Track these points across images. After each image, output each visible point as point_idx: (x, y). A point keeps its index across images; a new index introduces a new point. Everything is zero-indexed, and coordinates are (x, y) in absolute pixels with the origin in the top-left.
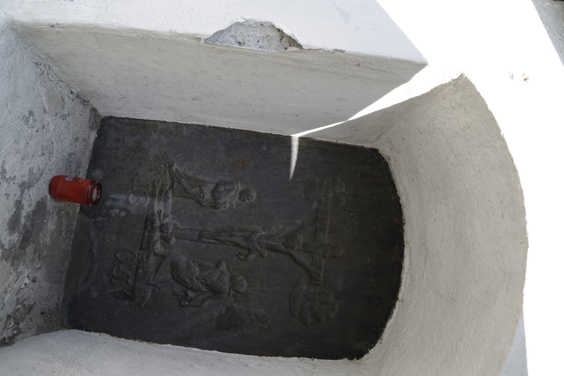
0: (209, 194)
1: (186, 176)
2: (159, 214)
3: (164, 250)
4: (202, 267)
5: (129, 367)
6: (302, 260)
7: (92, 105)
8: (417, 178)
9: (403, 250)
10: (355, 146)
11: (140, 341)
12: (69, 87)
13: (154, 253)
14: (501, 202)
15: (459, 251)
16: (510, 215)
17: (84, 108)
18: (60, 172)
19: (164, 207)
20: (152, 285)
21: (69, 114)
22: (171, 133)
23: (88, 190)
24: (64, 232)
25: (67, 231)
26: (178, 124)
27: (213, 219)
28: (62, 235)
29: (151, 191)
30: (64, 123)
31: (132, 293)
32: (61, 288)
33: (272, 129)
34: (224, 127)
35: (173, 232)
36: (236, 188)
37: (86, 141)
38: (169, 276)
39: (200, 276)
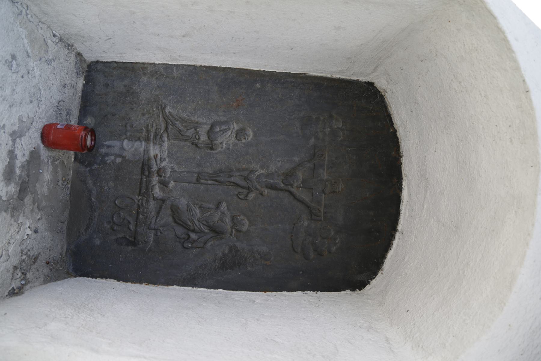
0: (204, 135)
1: (180, 118)
2: (155, 159)
3: (163, 194)
4: (202, 208)
5: (139, 309)
6: (303, 197)
7: (77, 49)
8: (416, 108)
9: (402, 182)
10: (350, 79)
11: (146, 285)
12: (51, 29)
13: (154, 197)
14: (510, 126)
15: (463, 179)
16: (519, 139)
17: (68, 52)
18: (51, 120)
19: (160, 150)
20: (154, 229)
21: (54, 59)
22: (161, 75)
23: (82, 136)
24: (61, 182)
25: (64, 181)
26: (167, 65)
27: (211, 160)
28: (59, 185)
29: (146, 136)
30: (50, 68)
31: (135, 238)
32: (63, 237)
33: (265, 66)
34: (216, 66)
35: (170, 176)
36: (232, 127)
37: (74, 88)
38: (171, 219)
39: (201, 218)
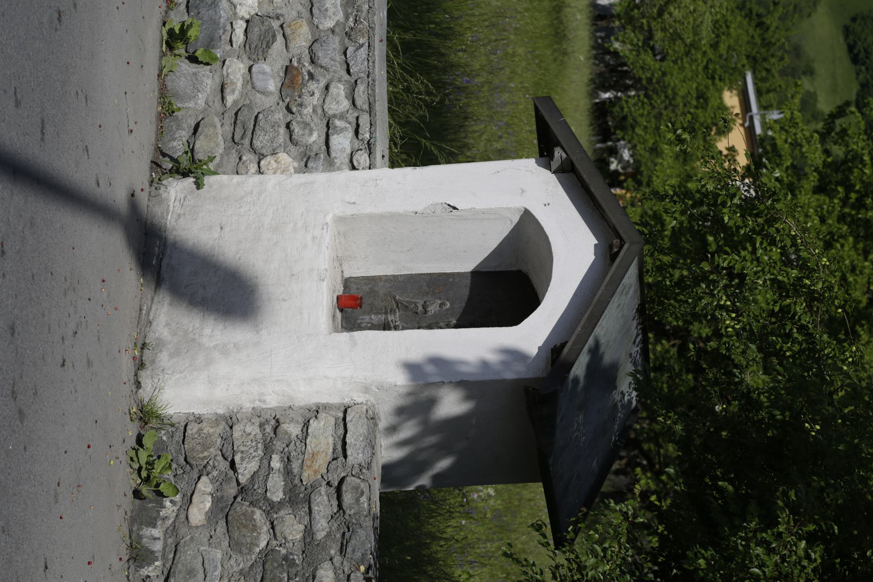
22: (391, 281)
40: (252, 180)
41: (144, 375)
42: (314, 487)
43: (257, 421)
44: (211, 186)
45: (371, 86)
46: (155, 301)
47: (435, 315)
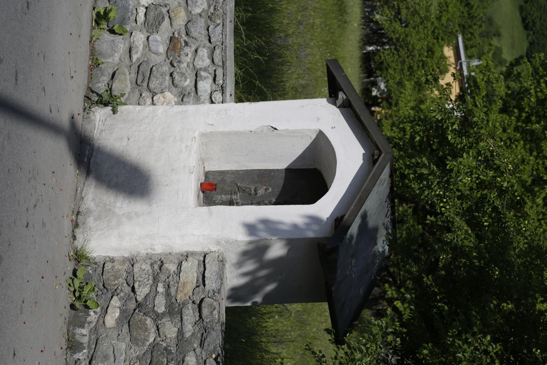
40: (148, 109)
41: (77, 231)
42: (184, 304)
43: (149, 262)
44: (122, 113)
45: (224, 50)
46: (86, 185)
47: (262, 196)
